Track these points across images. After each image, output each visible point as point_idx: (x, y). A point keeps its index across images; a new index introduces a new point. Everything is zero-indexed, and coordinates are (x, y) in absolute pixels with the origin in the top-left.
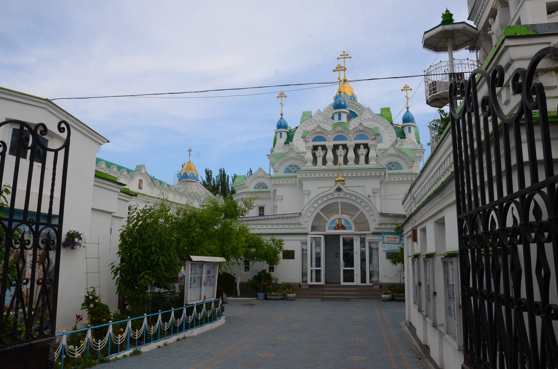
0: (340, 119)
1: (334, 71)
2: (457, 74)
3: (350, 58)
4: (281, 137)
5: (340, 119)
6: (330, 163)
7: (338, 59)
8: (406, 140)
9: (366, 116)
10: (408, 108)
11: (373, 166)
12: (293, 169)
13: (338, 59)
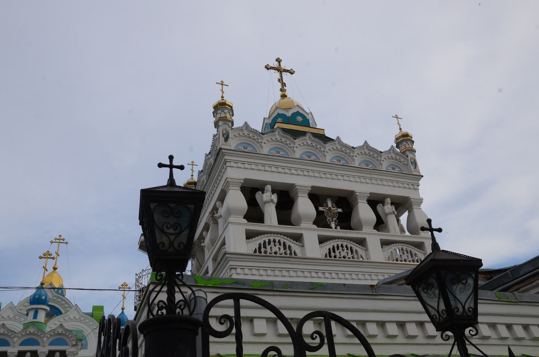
0: (35, 317)
1: (41, 258)
3: (67, 243)
5: (35, 317)
7: (52, 242)
9: (72, 314)
10: (123, 309)
13: (52, 242)
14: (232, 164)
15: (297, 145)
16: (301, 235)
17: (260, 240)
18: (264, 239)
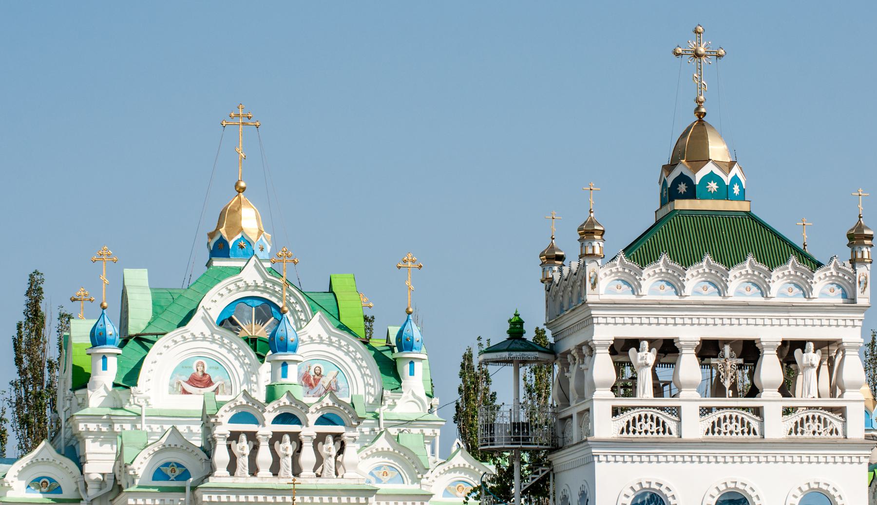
2: (523, 423)
4: (105, 368)
6: (264, 472)
8: (404, 395)
11: (352, 482)
12: (173, 471)
14: (601, 320)
15: (687, 276)
16: (678, 408)
17: (628, 416)
18: (633, 415)
